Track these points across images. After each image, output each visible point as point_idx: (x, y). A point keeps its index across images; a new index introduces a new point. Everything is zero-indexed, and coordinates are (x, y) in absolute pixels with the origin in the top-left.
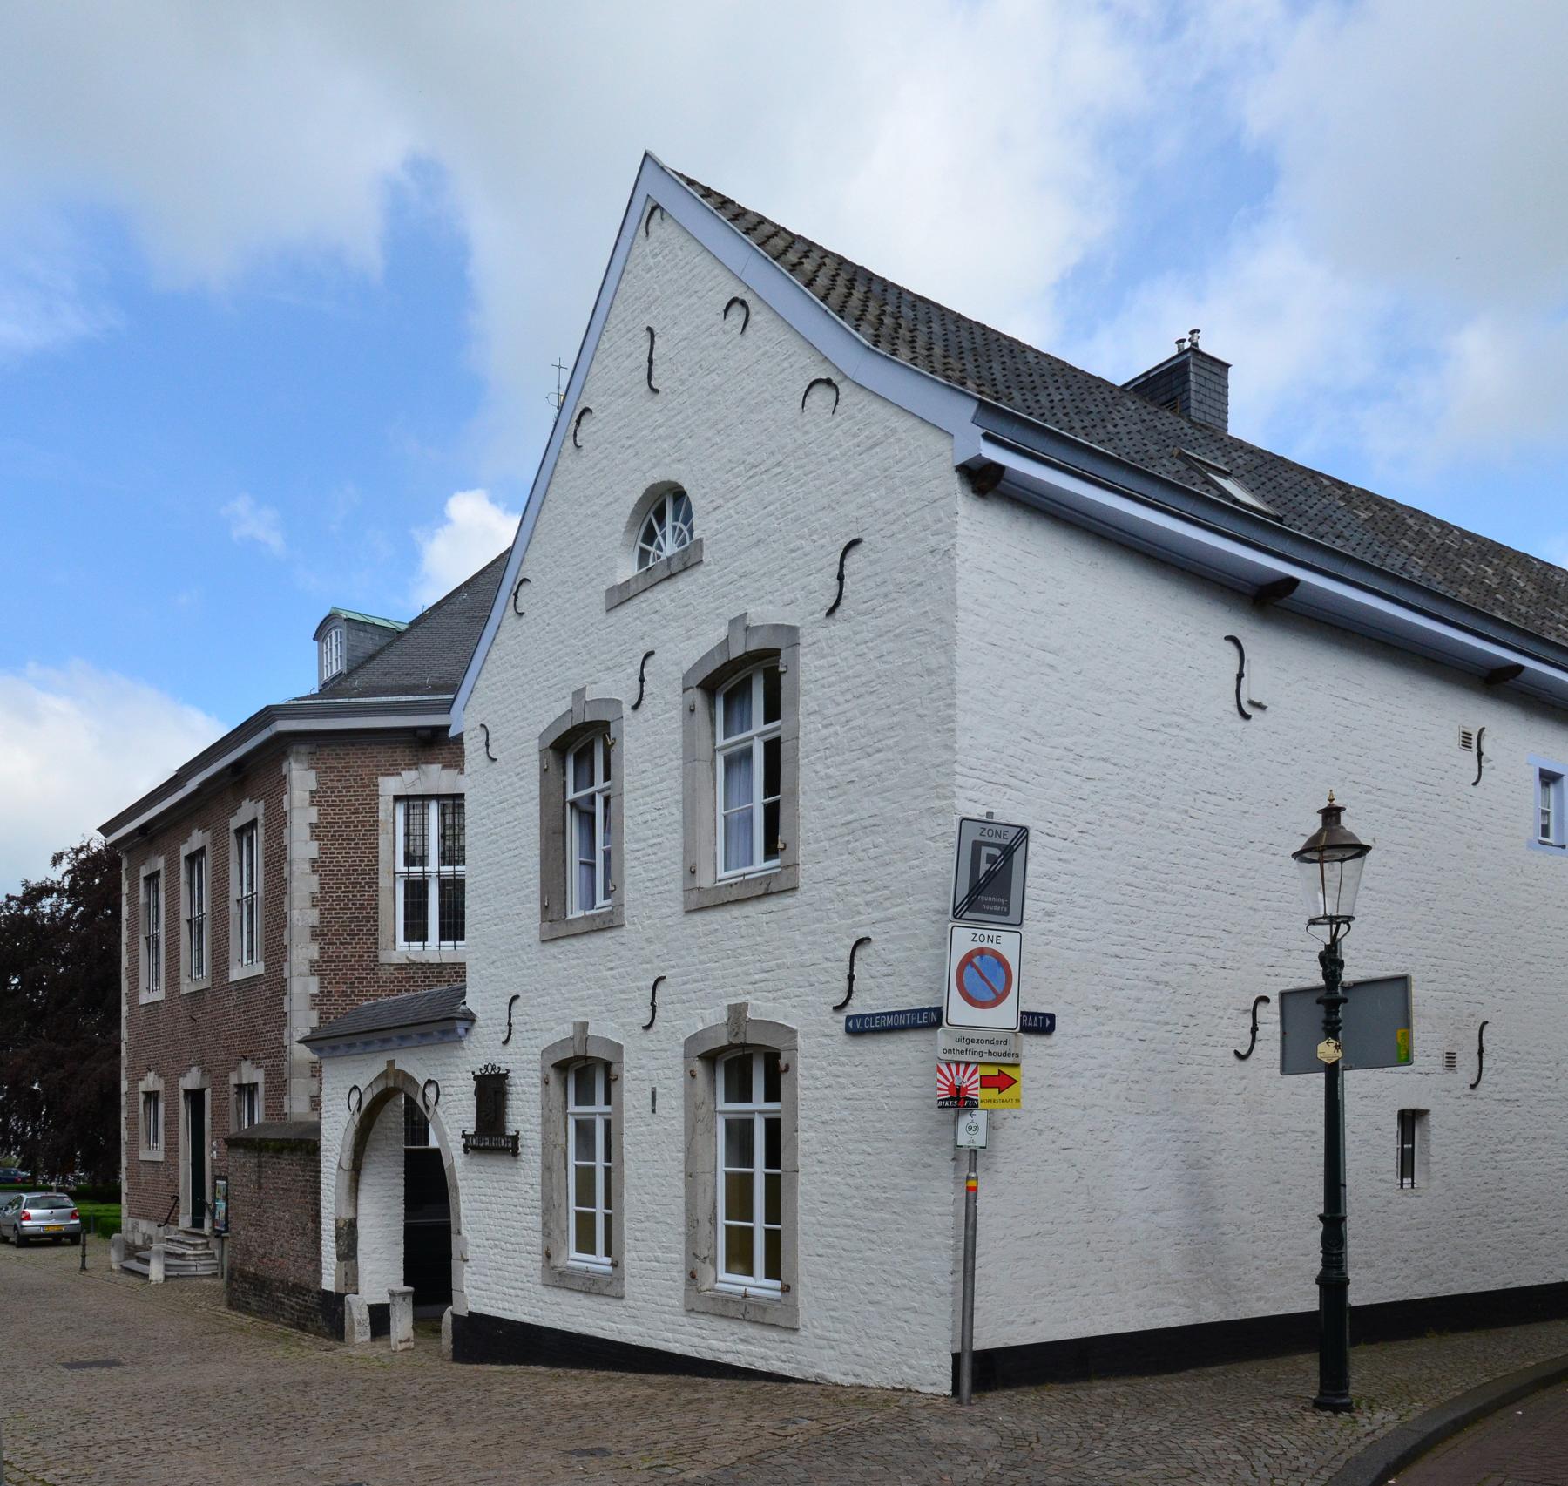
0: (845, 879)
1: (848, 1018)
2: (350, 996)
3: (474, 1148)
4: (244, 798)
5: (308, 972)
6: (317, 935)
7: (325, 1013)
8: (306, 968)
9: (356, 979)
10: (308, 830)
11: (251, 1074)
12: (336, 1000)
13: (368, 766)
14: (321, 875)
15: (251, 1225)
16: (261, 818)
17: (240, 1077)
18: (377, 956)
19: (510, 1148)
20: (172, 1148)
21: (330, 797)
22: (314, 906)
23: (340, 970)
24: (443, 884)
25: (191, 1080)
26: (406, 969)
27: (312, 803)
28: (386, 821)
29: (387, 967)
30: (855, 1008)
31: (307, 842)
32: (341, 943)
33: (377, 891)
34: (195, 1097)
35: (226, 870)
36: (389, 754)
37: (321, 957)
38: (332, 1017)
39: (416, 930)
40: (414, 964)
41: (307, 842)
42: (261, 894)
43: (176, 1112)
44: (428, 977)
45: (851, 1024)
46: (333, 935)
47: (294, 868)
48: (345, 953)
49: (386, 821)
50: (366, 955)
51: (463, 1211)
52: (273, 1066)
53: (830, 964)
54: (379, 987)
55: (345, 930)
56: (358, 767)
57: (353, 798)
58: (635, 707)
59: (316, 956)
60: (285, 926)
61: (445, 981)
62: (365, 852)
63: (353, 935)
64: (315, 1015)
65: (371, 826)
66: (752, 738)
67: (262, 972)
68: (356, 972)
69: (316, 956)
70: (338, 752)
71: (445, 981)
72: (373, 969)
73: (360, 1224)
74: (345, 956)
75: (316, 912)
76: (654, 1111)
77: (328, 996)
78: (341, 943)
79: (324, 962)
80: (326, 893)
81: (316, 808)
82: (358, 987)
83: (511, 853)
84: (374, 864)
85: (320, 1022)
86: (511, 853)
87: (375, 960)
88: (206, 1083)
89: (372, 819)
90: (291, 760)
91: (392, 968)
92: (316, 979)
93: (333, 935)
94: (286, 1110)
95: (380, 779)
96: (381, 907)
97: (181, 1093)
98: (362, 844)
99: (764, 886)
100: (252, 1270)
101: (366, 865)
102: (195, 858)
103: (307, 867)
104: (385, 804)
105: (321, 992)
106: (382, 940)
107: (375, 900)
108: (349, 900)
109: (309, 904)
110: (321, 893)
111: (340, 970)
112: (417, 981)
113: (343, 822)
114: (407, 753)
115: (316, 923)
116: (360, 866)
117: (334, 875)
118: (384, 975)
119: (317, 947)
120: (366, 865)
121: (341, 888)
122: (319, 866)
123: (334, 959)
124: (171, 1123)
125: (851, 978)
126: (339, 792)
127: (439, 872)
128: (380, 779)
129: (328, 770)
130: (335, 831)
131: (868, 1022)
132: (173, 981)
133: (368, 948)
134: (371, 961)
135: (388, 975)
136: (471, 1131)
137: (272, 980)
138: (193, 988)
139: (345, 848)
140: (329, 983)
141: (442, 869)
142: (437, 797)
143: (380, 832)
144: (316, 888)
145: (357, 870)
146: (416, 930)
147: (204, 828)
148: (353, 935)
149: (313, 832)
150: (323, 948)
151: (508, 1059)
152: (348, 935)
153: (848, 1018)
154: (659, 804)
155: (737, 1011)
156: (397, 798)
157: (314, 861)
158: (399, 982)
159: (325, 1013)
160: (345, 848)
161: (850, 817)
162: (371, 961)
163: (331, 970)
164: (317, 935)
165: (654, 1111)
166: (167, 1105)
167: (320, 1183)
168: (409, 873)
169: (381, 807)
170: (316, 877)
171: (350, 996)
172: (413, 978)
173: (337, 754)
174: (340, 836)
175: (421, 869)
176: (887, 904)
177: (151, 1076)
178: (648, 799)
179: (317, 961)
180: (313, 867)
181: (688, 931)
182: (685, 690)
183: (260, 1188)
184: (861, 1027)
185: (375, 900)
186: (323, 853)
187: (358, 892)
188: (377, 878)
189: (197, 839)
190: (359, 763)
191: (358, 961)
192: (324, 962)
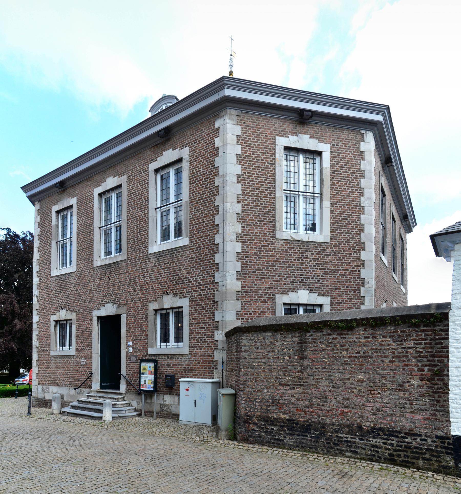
2: (259, 256)
6: (240, 219)
7: (245, 264)
8: (234, 237)
9: (262, 246)
10: (235, 158)
12: (250, 257)
13: (270, 129)
14: (242, 185)
21: (248, 141)
22: (238, 202)
23: (253, 240)
26: (289, 243)
29: (279, 241)
31: (235, 165)
32: (254, 225)
33: (274, 198)
36: (281, 125)
37: (242, 232)
38: (249, 266)
44: (302, 248)
46: (249, 220)
47: (228, 178)
48: (256, 231)
49: (280, 159)
50: (268, 233)
54: (275, 251)
55: (256, 218)
56: (264, 129)
57: (261, 144)
59: (240, 231)
61: (310, 251)
62: (267, 176)
63: (260, 221)
64: (239, 264)
65: (271, 161)
67: (188, 244)
69: (240, 231)
70: (253, 118)
71: (310, 251)
72: (272, 242)
74: (256, 233)
75: (240, 205)
78: (254, 225)
79: (244, 235)
80: (246, 195)
81: (240, 146)
82: (263, 251)
84: (273, 183)
85: (242, 269)
87: (273, 237)
89: (271, 157)
90: (226, 118)
91: (282, 242)
92: (240, 244)
93: (249, 220)
95: (277, 138)
96: (277, 207)
101: (268, 183)
103: (235, 179)
105: (242, 252)
106: (277, 226)
107: (273, 203)
108: (258, 201)
109: (236, 201)
110: (242, 195)
111: (253, 240)
112: (295, 250)
113: (255, 157)
114: (291, 126)
115: (240, 212)
116: (265, 182)
117: (250, 186)
118: (278, 245)
119: (241, 226)
120: (268, 183)
122: (241, 180)
123: (250, 234)
126: (253, 139)
128: (277, 138)
129: (248, 128)
130: (250, 161)
133: (269, 229)
134: (271, 237)
135: (280, 246)
139: (256, 172)
140: (247, 247)
143: (277, 165)
145: (263, 185)
150: (243, 227)
152: (258, 221)
157: (238, 176)
158: (286, 250)
159: (245, 264)
160: (256, 172)
162: (271, 237)
163: (248, 240)
164: (240, 219)
169: (277, 151)
170: (240, 185)
171: (259, 256)
172: (293, 248)
173: (252, 119)
174: (253, 164)
179: (240, 234)
180: (238, 179)
185: (273, 203)
186: (244, 173)
187: (263, 197)
190: (265, 127)
191: (263, 236)
192: (244, 235)
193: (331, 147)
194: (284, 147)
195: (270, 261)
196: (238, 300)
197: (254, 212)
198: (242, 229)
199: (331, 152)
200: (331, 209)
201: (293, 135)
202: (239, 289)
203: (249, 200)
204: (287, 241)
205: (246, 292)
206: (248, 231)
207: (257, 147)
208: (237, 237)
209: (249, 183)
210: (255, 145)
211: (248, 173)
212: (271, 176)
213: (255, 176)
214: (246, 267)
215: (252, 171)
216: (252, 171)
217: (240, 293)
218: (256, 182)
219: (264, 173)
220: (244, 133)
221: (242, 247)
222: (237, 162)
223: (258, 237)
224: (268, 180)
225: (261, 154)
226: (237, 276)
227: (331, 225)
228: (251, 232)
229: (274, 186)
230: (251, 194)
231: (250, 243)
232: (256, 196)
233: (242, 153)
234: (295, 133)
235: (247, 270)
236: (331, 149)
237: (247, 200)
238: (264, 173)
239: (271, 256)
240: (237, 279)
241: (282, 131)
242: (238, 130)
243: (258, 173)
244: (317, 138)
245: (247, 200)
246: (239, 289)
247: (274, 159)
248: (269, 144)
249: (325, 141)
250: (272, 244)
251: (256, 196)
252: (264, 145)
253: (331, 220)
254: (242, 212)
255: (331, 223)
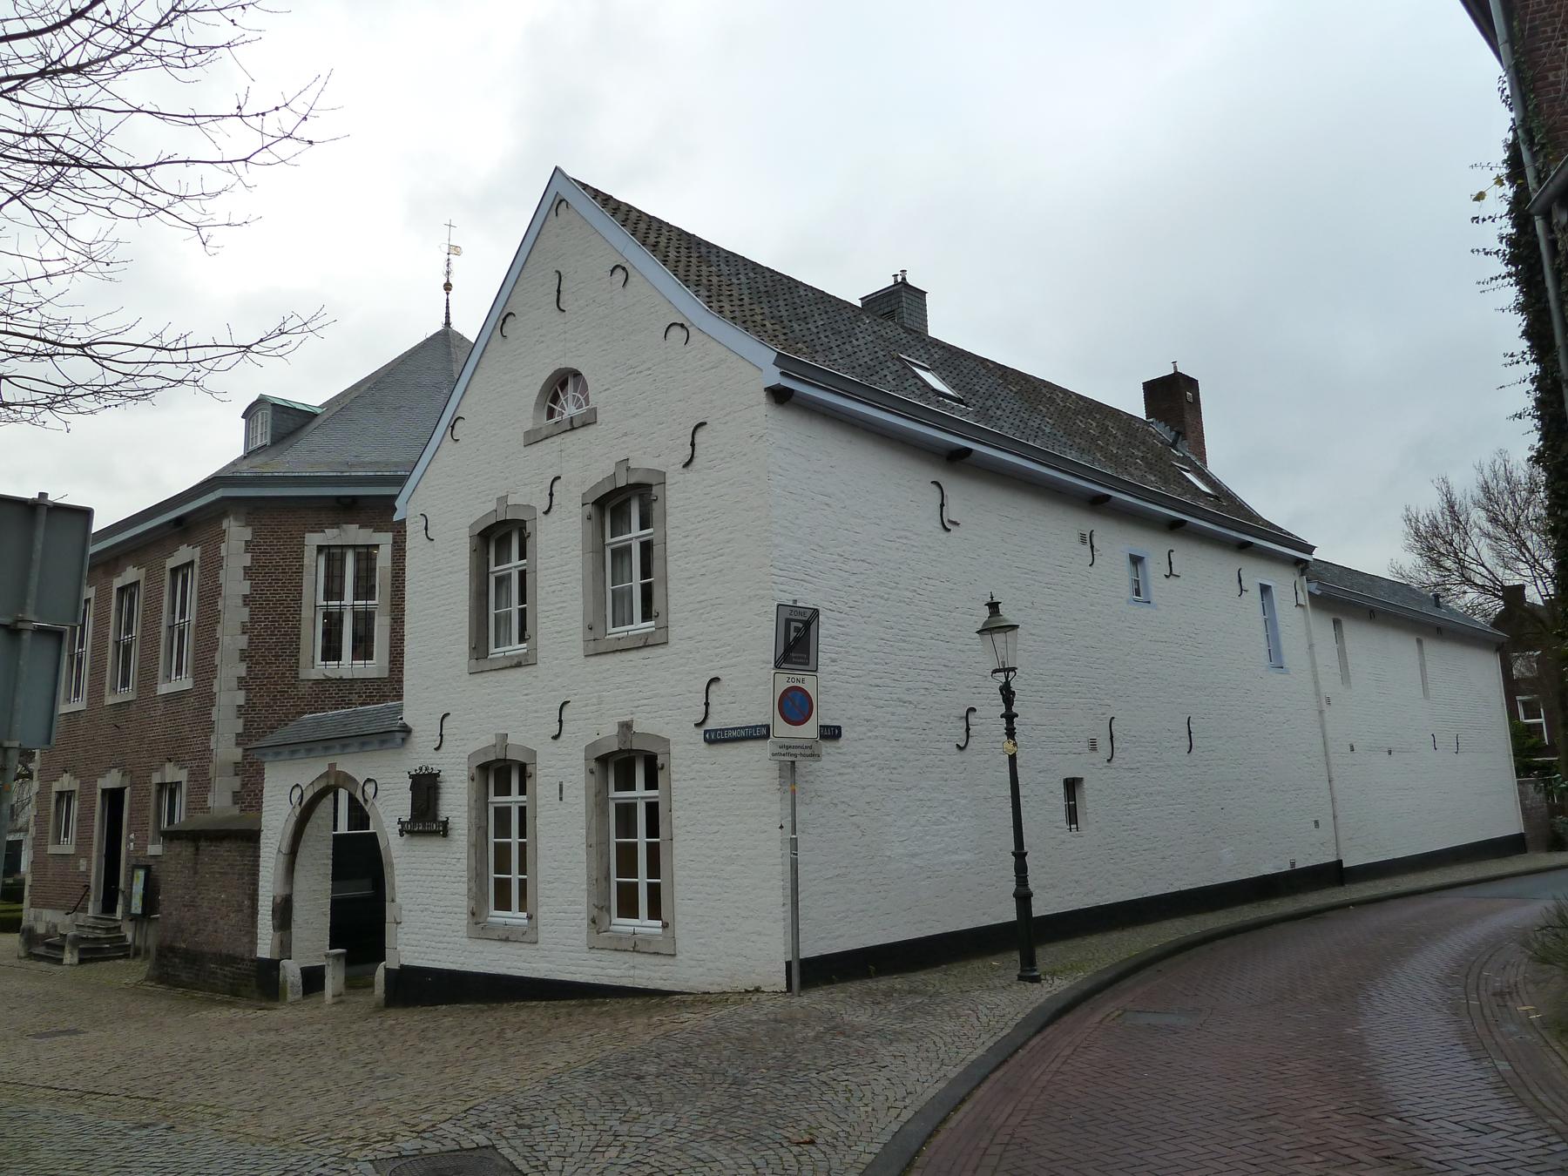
0: (701, 638)
1: (706, 732)
2: (272, 706)
3: (412, 833)
4: (182, 544)
5: (236, 687)
6: (245, 656)
7: (250, 721)
11: (173, 773)
14: (251, 608)
15: (185, 906)
16: (197, 560)
17: (163, 776)
18: (297, 674)
19: (443, 830)
20: (84, 842)
22: (244, 633)
24: (356, 615)
25: (112, 780)
27: (246, 551)
28: (311, 565)
30: (710, 726)
31: (240, 582)
32: (267, 663)
33: (300, 621)
34: (114, 798)
35: (159, 601)
37: (248, 675)
39: (332, 651)
40: (329, 679)
41: (240, 582)
42: (193, 622)
43: (92, 810)
45: (707, 736)
51: (397, 883)
52: (197, 766)
53: (691, 695)
54: (298, 698)
58: (546, 513)
60: (217, 649)
61: (356, 693)
63: (277, 656)
66: (631, 539)
68: (278, 687)
69: (244, 674)
71: (356, 693)
73: (295, 898)
74: (270, 674)
75: (246, 637)
76: (561, 799)
77: (253, 707)
78: (267, 663)
79: (251, 678)
83: (443, 608)
85: (245, 729)
86: (443, 608)
88: (127, 782)
90: (231, 518)
91: (310, 683)
94: (210, 804)
95: (307, 535)
97: (99, 792)
98: (289, 583)
99: (643, 640)
100: (184, 946)
102: (127, 591)
103: (240, 602)
104: (310, 554)
105: (247, 704)
107: (297, 628)
115: (245, 647)
121: (268, 618)
124: (85, 819)
125: (707, 704)
127: (353, 605)
128: (307, 535)
131: (720, 734)
132: (96, 693)
134: (292, 677)
135: (307, 689)
136: (406, 818)
137: (200, 694)
138: (118, 700)
141: (356, 603)
142: (354, 547)
143: (304, 574)
144: (246, 619)
146: (332, 651)
147: (139, 565)
148: (277, 656)
149: (245, 573)
151: (438, 761)
152: (273, 656)
153: (706, 732)
154: (563, 580)
155: (626, 727)
156: (320, 549)
157: (245, 596)
159: (250, 721)
161: (703, 598)
162: (292, 677)
165: (561, 799)
166: (81, 804)
167: (258, 866)
168: (327, 606)
172: (329, 690)
175: (338, 603)
176: (729, 656)
177: (66, 778)
178: (555, 576)
180: (245, 601)
181: (588, 669)
182: (583, 505)
183: (196, 873)
184: (715, 738)
185: (297, 628)
188: (300, 611)
189: (131, 574)
192: (251, 678)
193: (394, 536)
194: (318, 546)
195: (289, 713)
196: (237, 775)
197: (267, 645)
198: (248, 671)
199: (394, 542)
200: (391, 626)
201: (333, 528)
202: (239, 758)
203: (261, 629)
204: (317, 682)
205: (249, 763)
206: (257, 672)
207: (276, 553)
208: (239, 683)
209: (262, 604)
210: (273, 549)
211: (261, 590)
212: (295, 590)
213: (271, 594)
214: (251, 725)
215: (267, 587)
216: (267, 587)
217: (240, 765)
218: (273, 601)
219: (285, 587)
220: (258, 535)
221: (247, 696)
222: (245, 576)
223: (272, 680)
224: (291, 595)
225: (282, 561)
226: (237, 740)
227: (391, 651)
228: (262, 674)
229: (301, 603)
230: (265, 618)
231: (260, 689)
232: (272, 621)
233: (252, 563)
234: (335, 525)
235: (254, 729)
236: (394, 539)
237: (256, 629)
238: (285, 587)
239: (291, 706)
240: (238, 744)
241: (316, 524)
242: (247, 534)
243: (276, 588)
244: (371, 527)
245: (256, 629)
246: (239, 758)
247: (302, 565)
248: (294, 545)
249: (385, 528)
250: (294, 688)
251: (272, 621)
252: (286, 548)
253: (391, 643)
254: (249, 647)
255: (391, 647)
